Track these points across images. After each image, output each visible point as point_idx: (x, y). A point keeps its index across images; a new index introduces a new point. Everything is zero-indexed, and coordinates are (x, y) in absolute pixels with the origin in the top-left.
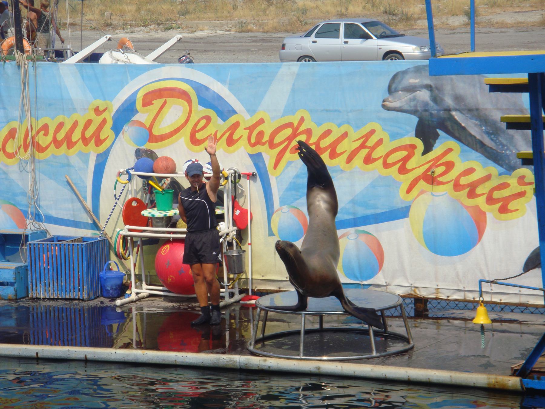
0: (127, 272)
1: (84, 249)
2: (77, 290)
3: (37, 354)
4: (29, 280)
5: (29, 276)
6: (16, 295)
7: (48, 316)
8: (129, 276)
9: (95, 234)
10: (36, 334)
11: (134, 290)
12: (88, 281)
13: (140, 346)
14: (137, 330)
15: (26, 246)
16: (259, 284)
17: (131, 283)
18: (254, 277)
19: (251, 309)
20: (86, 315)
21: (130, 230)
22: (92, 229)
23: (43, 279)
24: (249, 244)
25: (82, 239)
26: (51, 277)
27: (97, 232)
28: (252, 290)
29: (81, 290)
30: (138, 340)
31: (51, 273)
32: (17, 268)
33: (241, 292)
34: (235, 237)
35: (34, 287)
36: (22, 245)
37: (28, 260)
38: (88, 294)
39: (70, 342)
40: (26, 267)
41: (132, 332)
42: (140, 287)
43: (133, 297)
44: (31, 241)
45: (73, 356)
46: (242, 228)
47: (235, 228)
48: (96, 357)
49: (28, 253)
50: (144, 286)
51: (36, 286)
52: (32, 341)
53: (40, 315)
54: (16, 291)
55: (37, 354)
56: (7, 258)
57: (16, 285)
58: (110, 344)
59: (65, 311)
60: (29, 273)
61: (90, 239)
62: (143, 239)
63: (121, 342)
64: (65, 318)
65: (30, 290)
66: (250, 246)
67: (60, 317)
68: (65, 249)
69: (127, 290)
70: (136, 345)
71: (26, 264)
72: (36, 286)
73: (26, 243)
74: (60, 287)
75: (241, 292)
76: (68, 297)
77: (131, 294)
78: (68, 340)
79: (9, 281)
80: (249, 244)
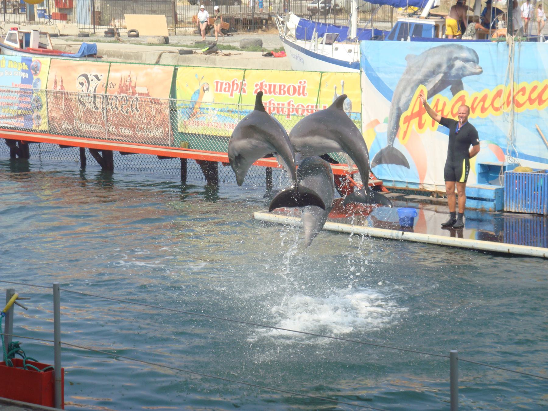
2: (539, 207)
4: (505, 198)
5: (505, 196)
6: (495, 209)
7: (517, 224)
10: (508, 236)
23: (515, 198)
26: (521, 197)
32: (497, 189)
35: (508, 204)
37: (505, 184)
40: (503, 189)
49: (505, 179)
54: (495, 205)
56: (490, 182)
57: (495, 201)
59: (529, 222)
60: (505, 193)
64: (529, 226)
65: (505, 206)
71: (503, 187)
74: (527, 205)
76: (532, 212)
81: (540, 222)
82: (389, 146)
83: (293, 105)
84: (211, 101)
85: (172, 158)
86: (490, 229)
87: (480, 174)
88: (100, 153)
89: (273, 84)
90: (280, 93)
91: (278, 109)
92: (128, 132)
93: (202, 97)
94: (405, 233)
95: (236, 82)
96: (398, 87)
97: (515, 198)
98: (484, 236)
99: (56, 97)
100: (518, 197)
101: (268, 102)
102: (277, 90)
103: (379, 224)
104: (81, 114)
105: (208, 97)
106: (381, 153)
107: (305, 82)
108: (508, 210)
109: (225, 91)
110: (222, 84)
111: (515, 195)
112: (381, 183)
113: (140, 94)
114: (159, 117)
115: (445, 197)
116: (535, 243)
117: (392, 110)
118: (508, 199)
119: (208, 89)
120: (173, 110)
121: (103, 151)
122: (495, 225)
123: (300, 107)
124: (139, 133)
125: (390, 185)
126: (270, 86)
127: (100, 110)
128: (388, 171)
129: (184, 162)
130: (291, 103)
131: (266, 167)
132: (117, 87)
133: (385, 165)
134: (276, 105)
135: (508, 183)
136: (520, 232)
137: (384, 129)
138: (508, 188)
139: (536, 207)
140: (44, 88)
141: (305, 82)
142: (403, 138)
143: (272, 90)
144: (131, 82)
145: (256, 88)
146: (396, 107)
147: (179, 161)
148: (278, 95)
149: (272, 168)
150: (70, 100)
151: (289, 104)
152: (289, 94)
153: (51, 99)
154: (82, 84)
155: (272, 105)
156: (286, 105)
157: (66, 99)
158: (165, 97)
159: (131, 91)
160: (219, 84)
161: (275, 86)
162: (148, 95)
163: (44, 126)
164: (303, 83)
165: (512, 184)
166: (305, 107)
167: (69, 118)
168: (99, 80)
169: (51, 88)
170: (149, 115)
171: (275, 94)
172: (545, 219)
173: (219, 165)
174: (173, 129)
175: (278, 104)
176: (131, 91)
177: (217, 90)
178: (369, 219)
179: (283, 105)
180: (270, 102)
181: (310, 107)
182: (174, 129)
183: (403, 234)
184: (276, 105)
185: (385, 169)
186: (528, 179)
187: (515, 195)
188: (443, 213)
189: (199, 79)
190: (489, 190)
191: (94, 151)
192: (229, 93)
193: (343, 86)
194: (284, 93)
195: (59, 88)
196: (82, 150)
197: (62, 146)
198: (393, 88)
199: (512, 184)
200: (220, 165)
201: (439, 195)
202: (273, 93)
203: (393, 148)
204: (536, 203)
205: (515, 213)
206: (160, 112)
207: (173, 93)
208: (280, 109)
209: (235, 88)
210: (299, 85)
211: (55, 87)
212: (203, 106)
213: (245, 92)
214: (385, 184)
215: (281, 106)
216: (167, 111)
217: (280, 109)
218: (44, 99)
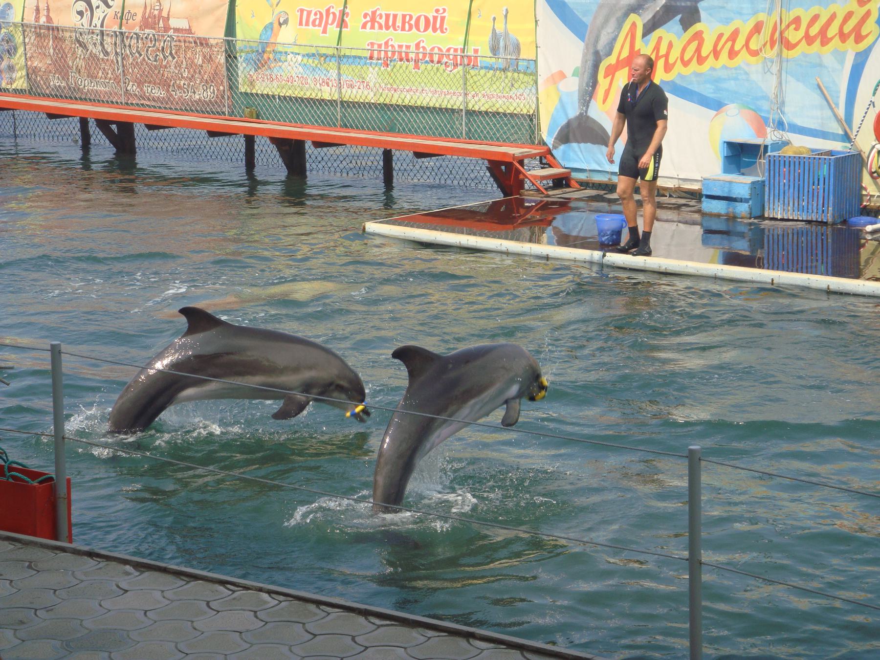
1: (832, 164)
2: (820, 211)
3: (773, 280)
6: (751, 214)
7: (786, 239)
9: (846, 147)
10: (771, 257)
20: (830, 240)
22: (844, 141)
25: (830, 153)
26: (791, 195)
27: (849, 145)
29: (826, 211)
31: (791, 190)
32: (753, 183)
35: (771, 206)
37: (767, 174)
38: (834, 217)
40: (763, 182)
45: (814, 285)
49: (767, 167)
52: (766, 266)
53: (776, 237)
54: (751, 209)
55: (773, 280)
56: (742, 170)
57: (751, 202)
58: (857, 274)
60: (767, 189)
61: (839, 152)
63: (868, 273)
64: (805, 242)
65: (767, 209)
67: (800, 241)
74: (801, 207)
78: (807, 268)
81: (822, 235)
82: (581, 114)
83: (424, 48)
84: (292, 41)
85: (230, 134)
86: (742, 247)
87: (727, 158)
88: (114, 127)
89: (392, 13)
90: (403, 29)
91: (400, 53)
92: (158, 93)
93: (276, 36)
94: (608, 254)
95: (332, 10)
96: (595, 18)
98: (732, 259)
99: (39, 35)
100: (787, 194)
101: (383, 42)
102: (399, 23)
103: (565, 240)
104: (81, 63)
105: (286, 36)
106: (568, 124)
107: (444, 10)
109: (314, 25)
110: (309, 13)
111: (782, 191)
112: (569, 173)
113: (177, 30)
114: (209, 68)
115: (671, 196)
116: (814, 269)
117: (585, 55)
118: (772, 198)
119: (286, 22)
120: (231, 57)
121: (120, 124)
122: (750, 241)
123: (436, 50)
124: (177, 94)
125: (582, 176)
126: (388, 16)
127: (112, 57)
128: (579, 153)
129: (250, 141)
130: (422, 44)
131: (383, 150)
132: (139, 18)
133: (575, 145)
134: (397, 49)
135: (772, 172)
136: (790, 251)
137: (572, 86)
138: (772, 181)
140: (18, 19)
141: (444, 10)
142: (604, 101)
143: (391, 23)
144: (161, 10)
145: (364, 20)
146: (592, 50)
147: (242, 140)
148: (399, 31)
149: (393, 151)
150: (63, 40)
151: (417, 45)
152: (418, 29)
153: (32, 38)
154: (81, 13)
155: (390, 48)
156: (413, 48)
157: (55, 38)
158: (218, 34)
159: (161, 24)
160: (305, 13)
161: (395, 16)
162: (189, 31)
163: (21, 83)
164: (441, 11)
165: (777, 175)
166: (444, 50)
167: (62, 69)
168: (109, 6)
169: (30, 19)
170: (191, 64)
171: (395, 29)
172: (830, 229)
173: (307, 147)
174: (231, 88)
175: (400, 46)
176: (161, 24)
177: (301, 24)
178: (549, 231)
179: (408, 47)
180: (386, 43)
181: (452, 50)
182: (232, 86)
183: (604, 256)
184: (397, 49)
185: (575, 152)
186: (804, 165)
187: (782, 191)
188: (667, 221)
189: (271, 6)
190: (742, 184)
191: (104, 124)
192: (321, 29)
193: (506, 16)
194: (410, 29)
195: (43, 20)
196: (84, 122)
197: (51, 116)
198: (587, 20)
199: (777, 175)
200: (308, 145)
201: (661, 192)
202: (391, 29)
203: (588, 117)
204: (815, 205)
205: (782, 220)
206: (209, 59)
207: (230, 29)
208: (403, 55)
209: (330, 22)
210: (436, 14)
211: (37, 19)
212: (280, 48)
213: (346, 27)
214: (574, 175)
215: (404, 49)
216: (221, 59)
217: (403, 55)
218: (19, 38)
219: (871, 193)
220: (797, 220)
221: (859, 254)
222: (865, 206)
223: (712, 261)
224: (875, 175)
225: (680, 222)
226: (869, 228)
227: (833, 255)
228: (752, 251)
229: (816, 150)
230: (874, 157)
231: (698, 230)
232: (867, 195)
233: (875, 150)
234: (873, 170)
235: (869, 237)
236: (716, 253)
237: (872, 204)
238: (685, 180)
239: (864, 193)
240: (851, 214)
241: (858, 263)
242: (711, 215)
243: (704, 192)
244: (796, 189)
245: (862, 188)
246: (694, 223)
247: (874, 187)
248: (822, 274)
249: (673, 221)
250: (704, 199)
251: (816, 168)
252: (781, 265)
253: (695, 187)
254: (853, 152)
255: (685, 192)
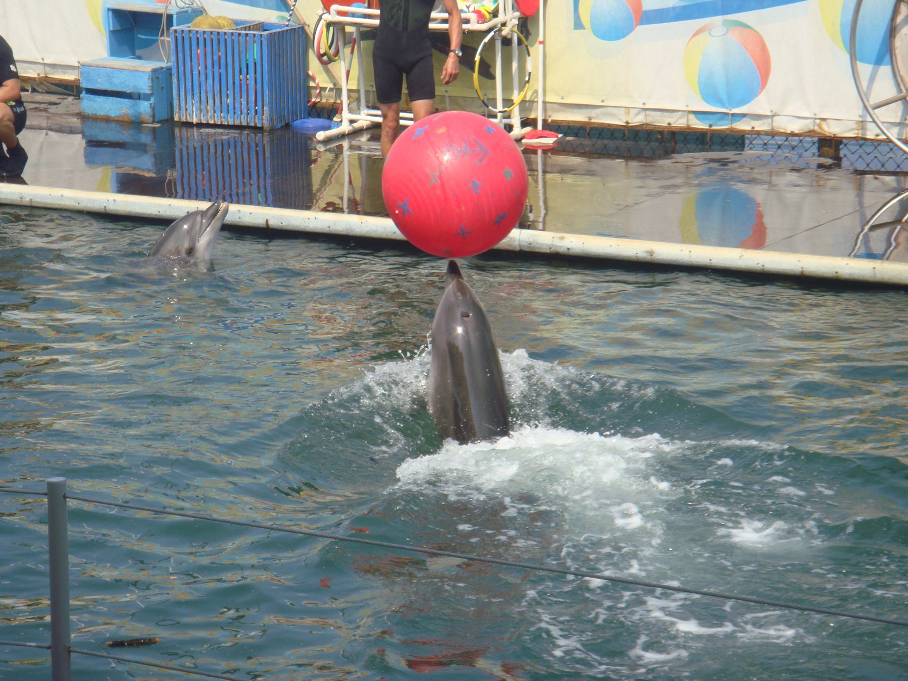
0: (335, 85)
1: (265, 43)
2: (252, 112)
4: (175, 92)
5: (175, 86)
6: (153, 116)
7: (205, 152)
8: (339, 91)
9: (283, 18)
10: (185, 181)
11: (346, 115)
12: (271, 98)
13: (354, 208)
14: (350, 182)
15: (168, 36)
16: (555, 111)
17: (341, 103)
18: (548, 99)
19: (540, 151)
20: (268, 154)
21: (340, 13)
22: (279, 9)
23: (196, 91)
24: (541, 43)
25: (261, 26)
26: (210, 88)
27: (286, 15)
28: (545, 121)
29: (260, 111)
30: (351, 196)
31: (210, 81)
32: (154, 71)
33: (525, 123)
34: (516, 29)
35: (183, 105)
36: (162, 35)
37: (173, 58)
38: (272, 120)
39: (241, 198)
40: (169, 69)
41: (343, 185)
42: (358, 111)
43: (345, 128)
44: (178, 25)
46: (528, 13)
47: (517, 14)
48: (284, 224)
49: (173, 46)
50: (365, 111)
51: (186, 103)
53: (191, 151)
54: (153, 108)
56: (138, 52)
57: (152, 99)
58: (305, 202)
59: (232, 146)
60: (175, 80)
61: (273, 26)
62: (362, 29)
64: (233, 157)
65: (176, 109)
66: (541, 46)
67: (226, 155)
68: (233, 41)
69: (334, 116)
70: (348, 208)
71: (170, 64)
72: (186, 103)
73: (168, 29)
74: (224, 106)
75: (525, 123)
76: (237, 123)
77: (341, 121)
78: (238, 194)
79: (142, 92)
80: (541, 43)
81: (257, 146)
86: (145, 166)
87: (113, 33)
97: (196, 91)
98: (130, 184)
100: (203, 89)
108: (183, 119)
111: (196, 83)
115: (34, 90)
118: (183, 97)
122: (155, 155)
135: (180, 55)
136: (213, 171)
138: (181, 68)
139: (245, 111)
165: (188, 58)
172: (266, 139)
186: (223, 44)
187: (196, 83)
190: (136, 71)
199: (188, 58)
204: (244, 103)
205: (200, 125)
219: (321, 85)
220: (221, 126)
221: (308, 173)
222: (315, 103)
223: (101, 188)
224: (325, 58)
225: (50, 129)
226: (321, 135)
227: (273, 175)
228: (158, 172)
229: (242, 22)
230: (321, 33)
231: (77, 142)
232: (316, 88)
233: (322, 22)
234: (322, 52)
235: (321, 148)
236: (106, 173)
237: (324, 101)
238: (53, 66)
239: (312, 84)
240: (295, 116)
241: (310, 185)
242: (95, 119)
243: (84, 85)
244: (217, 79)
245: (308, 77)
246: (72, 131)
247: (324, 75)
248: (259, 204)
249: (41, 128)
250: (83, 95)
251: (243, 49)
252: (200, 192)
253: (70, 77)
254: (295, 26)
255: (56, 85)
